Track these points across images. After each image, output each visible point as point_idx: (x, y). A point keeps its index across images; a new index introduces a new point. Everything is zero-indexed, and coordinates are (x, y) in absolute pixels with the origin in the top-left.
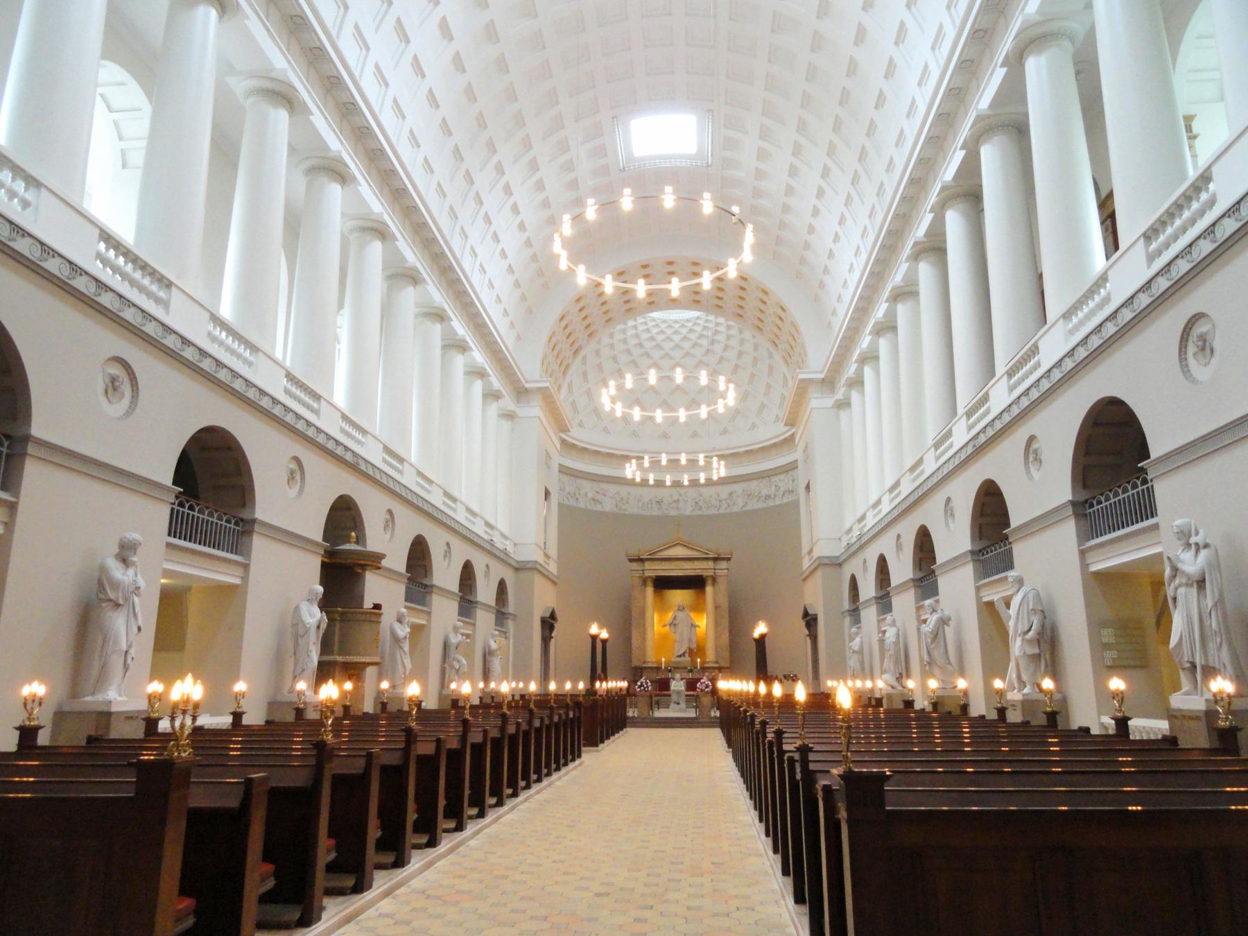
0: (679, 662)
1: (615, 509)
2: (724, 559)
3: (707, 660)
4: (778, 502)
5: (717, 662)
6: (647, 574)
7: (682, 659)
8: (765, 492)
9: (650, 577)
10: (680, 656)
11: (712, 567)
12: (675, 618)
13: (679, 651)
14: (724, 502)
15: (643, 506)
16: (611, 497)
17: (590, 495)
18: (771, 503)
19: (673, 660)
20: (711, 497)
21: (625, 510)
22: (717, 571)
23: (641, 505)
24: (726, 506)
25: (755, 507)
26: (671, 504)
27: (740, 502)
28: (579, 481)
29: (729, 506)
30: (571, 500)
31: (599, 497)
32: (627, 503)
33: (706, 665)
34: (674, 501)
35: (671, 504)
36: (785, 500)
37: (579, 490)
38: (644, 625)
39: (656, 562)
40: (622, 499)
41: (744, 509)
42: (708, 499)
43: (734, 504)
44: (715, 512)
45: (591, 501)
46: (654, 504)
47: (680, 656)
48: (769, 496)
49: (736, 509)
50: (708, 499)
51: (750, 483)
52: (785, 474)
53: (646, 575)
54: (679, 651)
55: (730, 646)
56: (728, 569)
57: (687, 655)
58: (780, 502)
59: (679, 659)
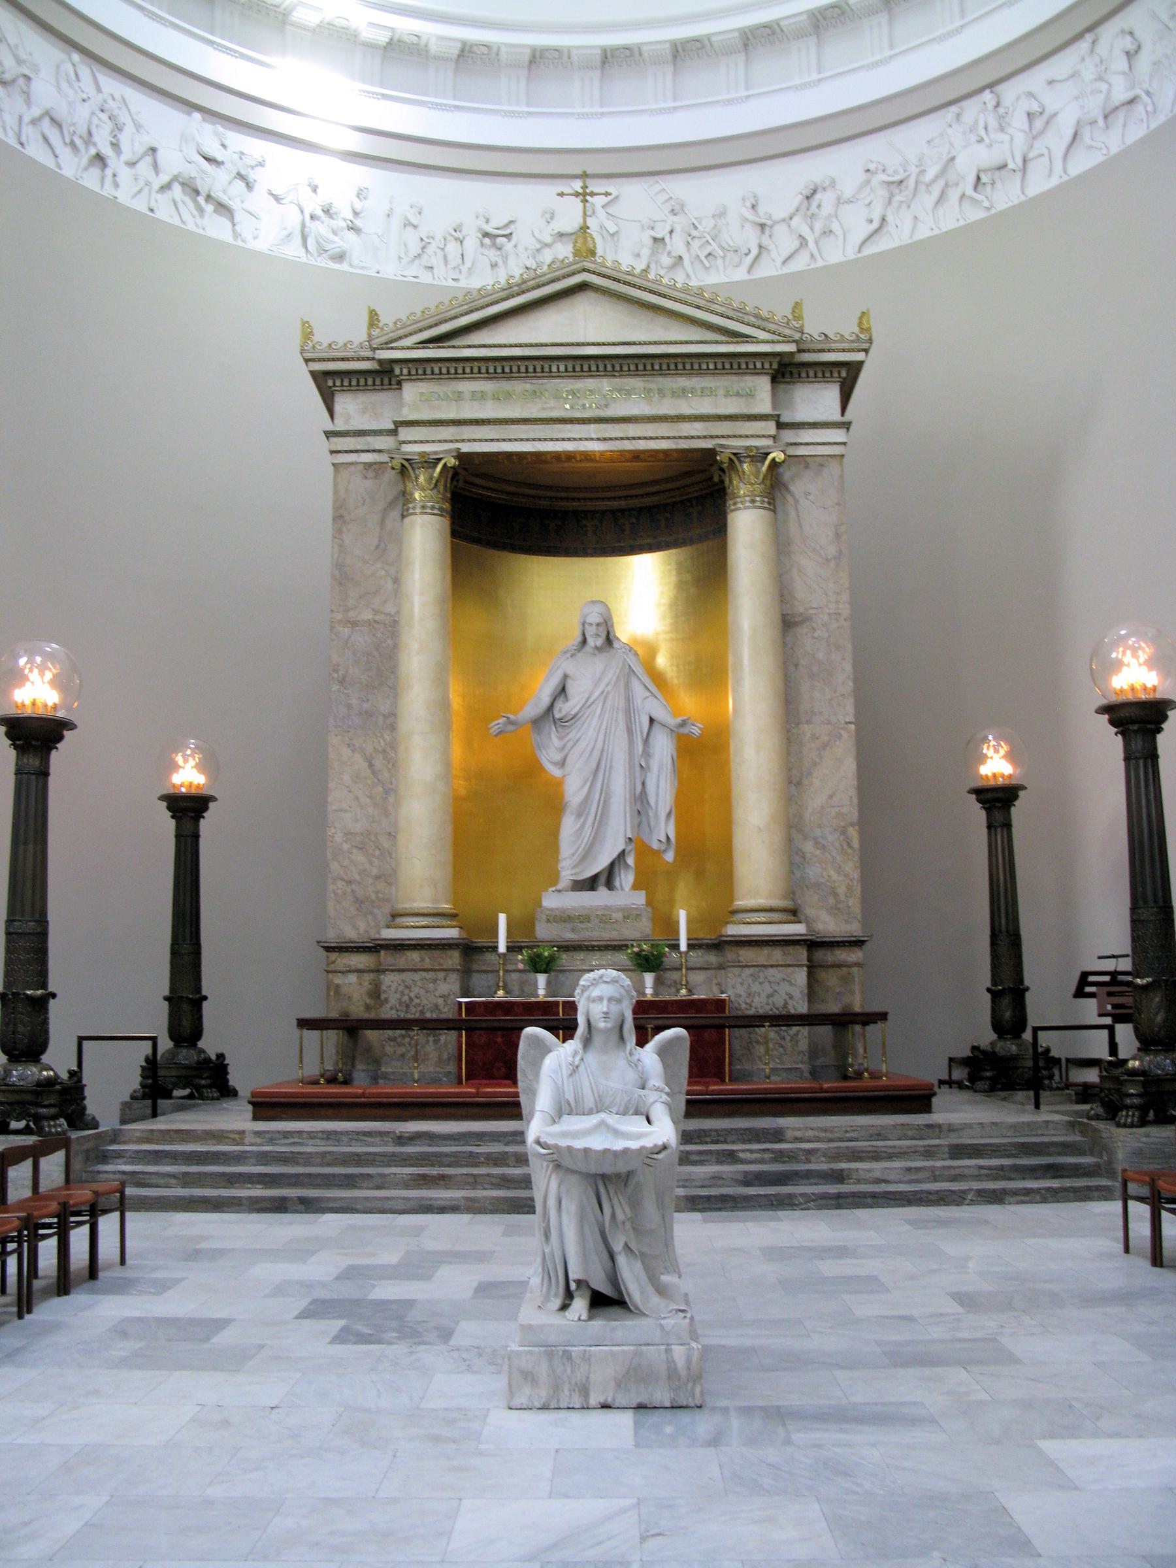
0: (583, 918)
1: (294, 251)
2: (824, 371)
3: (739, 903)
4: (1039, 183)
5: (793, 914)
6: (417, 443)
7: (600, 898)
8: (971, 158)
9: (430, 462)
10: (591, 884)
11: (765, 407)
12: (562, 691)
13: (588, 854)
14: (781, 231)
15: (424, 248)
16: (277, 199)
17: (173, 161)
18: (1007, 195)
19: (552, 901)
20: (722, 214)
21: (340, 257)
22: (789, 436)
23: (415, 248)
24: (789, 244)
25: (923, 233)
26: (547, 245)
27: (855, 223)
28: (112, 86)
29: (803, 241)
30: (65, 153)
31: (218, 181)
32: (352, 228)
33: (733, 930)
34: (561, 235)
35: (547, 245)
36: (1082, 163)
37: (118, 128)
38: (391, 722)
39: (466, 387)
40: (327, 211)
41: (871, 249)
42: (707, 225)
43: (827, 232)
44: (740, 274)
45: (177, 188)
46: (471, 243)
47: (591, 884)
48: (1004, 166)
49: (836, 253)
50: (707, 225)
51: (898, 136)
52: (1084, 45)
53: (407, 448)
54: (588, 854)
55: (863, 823)
56: (847, 426)
57: (626, 879)
58: (1055, 181)
59: (586, 900)
